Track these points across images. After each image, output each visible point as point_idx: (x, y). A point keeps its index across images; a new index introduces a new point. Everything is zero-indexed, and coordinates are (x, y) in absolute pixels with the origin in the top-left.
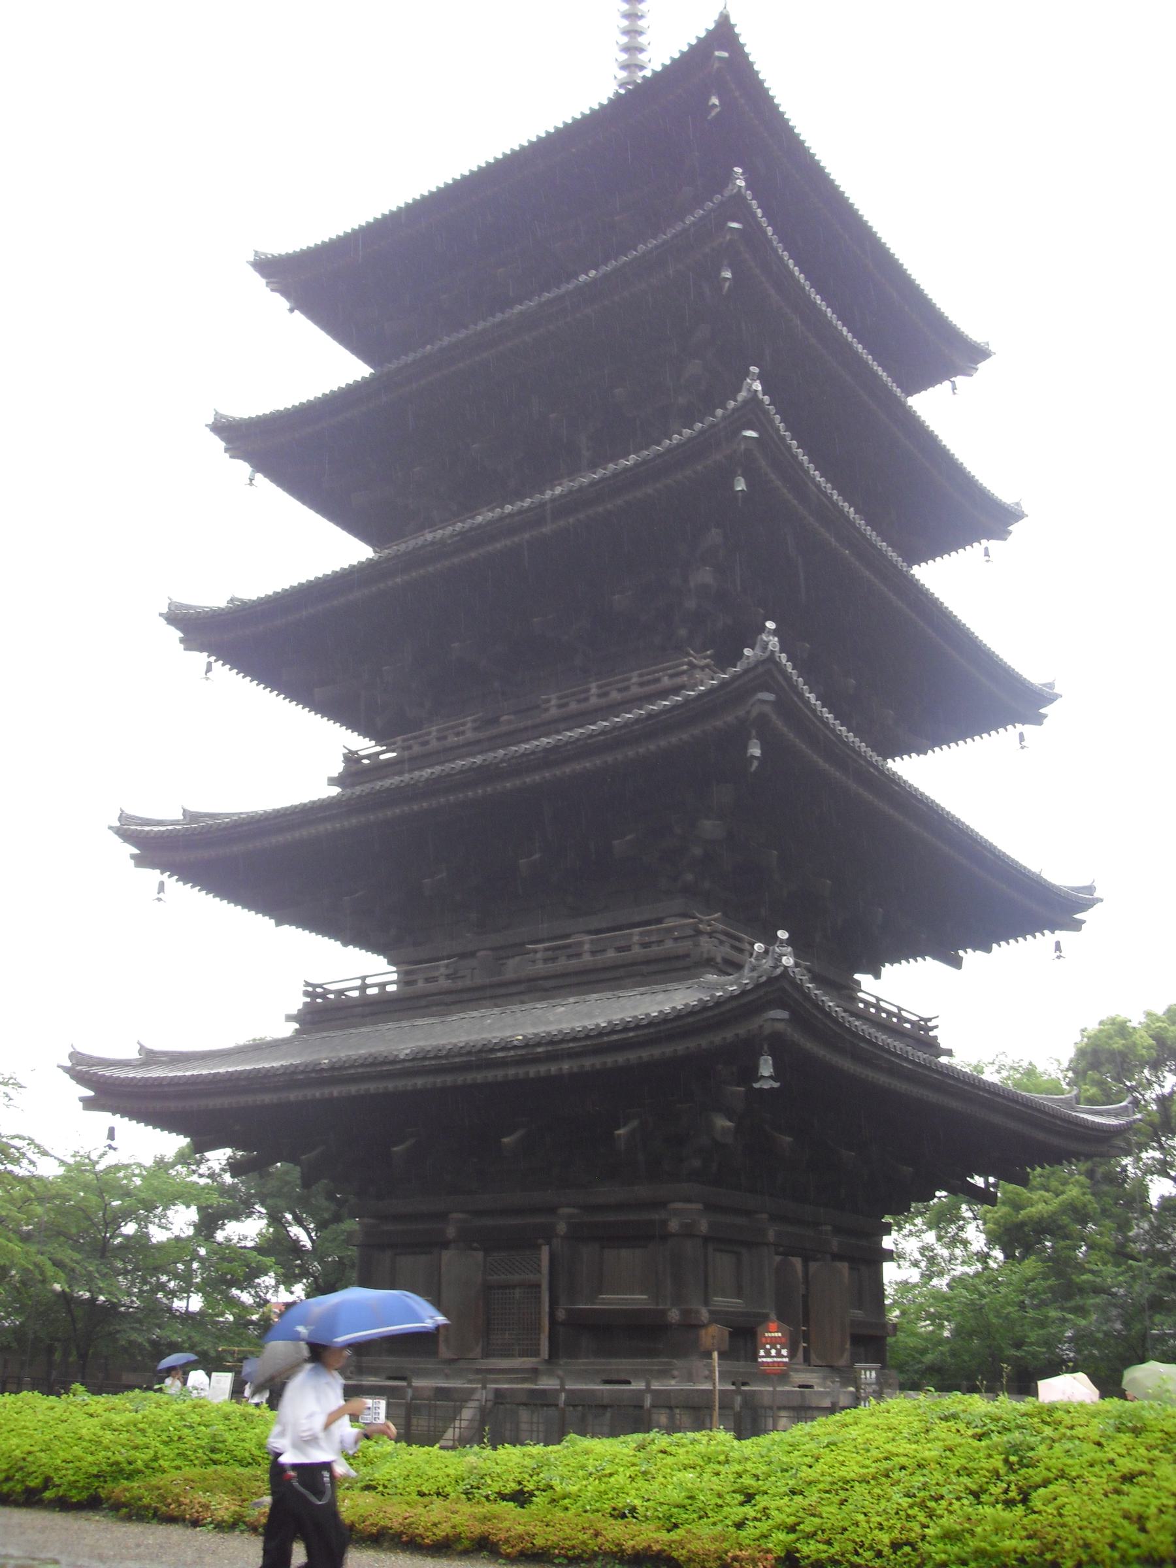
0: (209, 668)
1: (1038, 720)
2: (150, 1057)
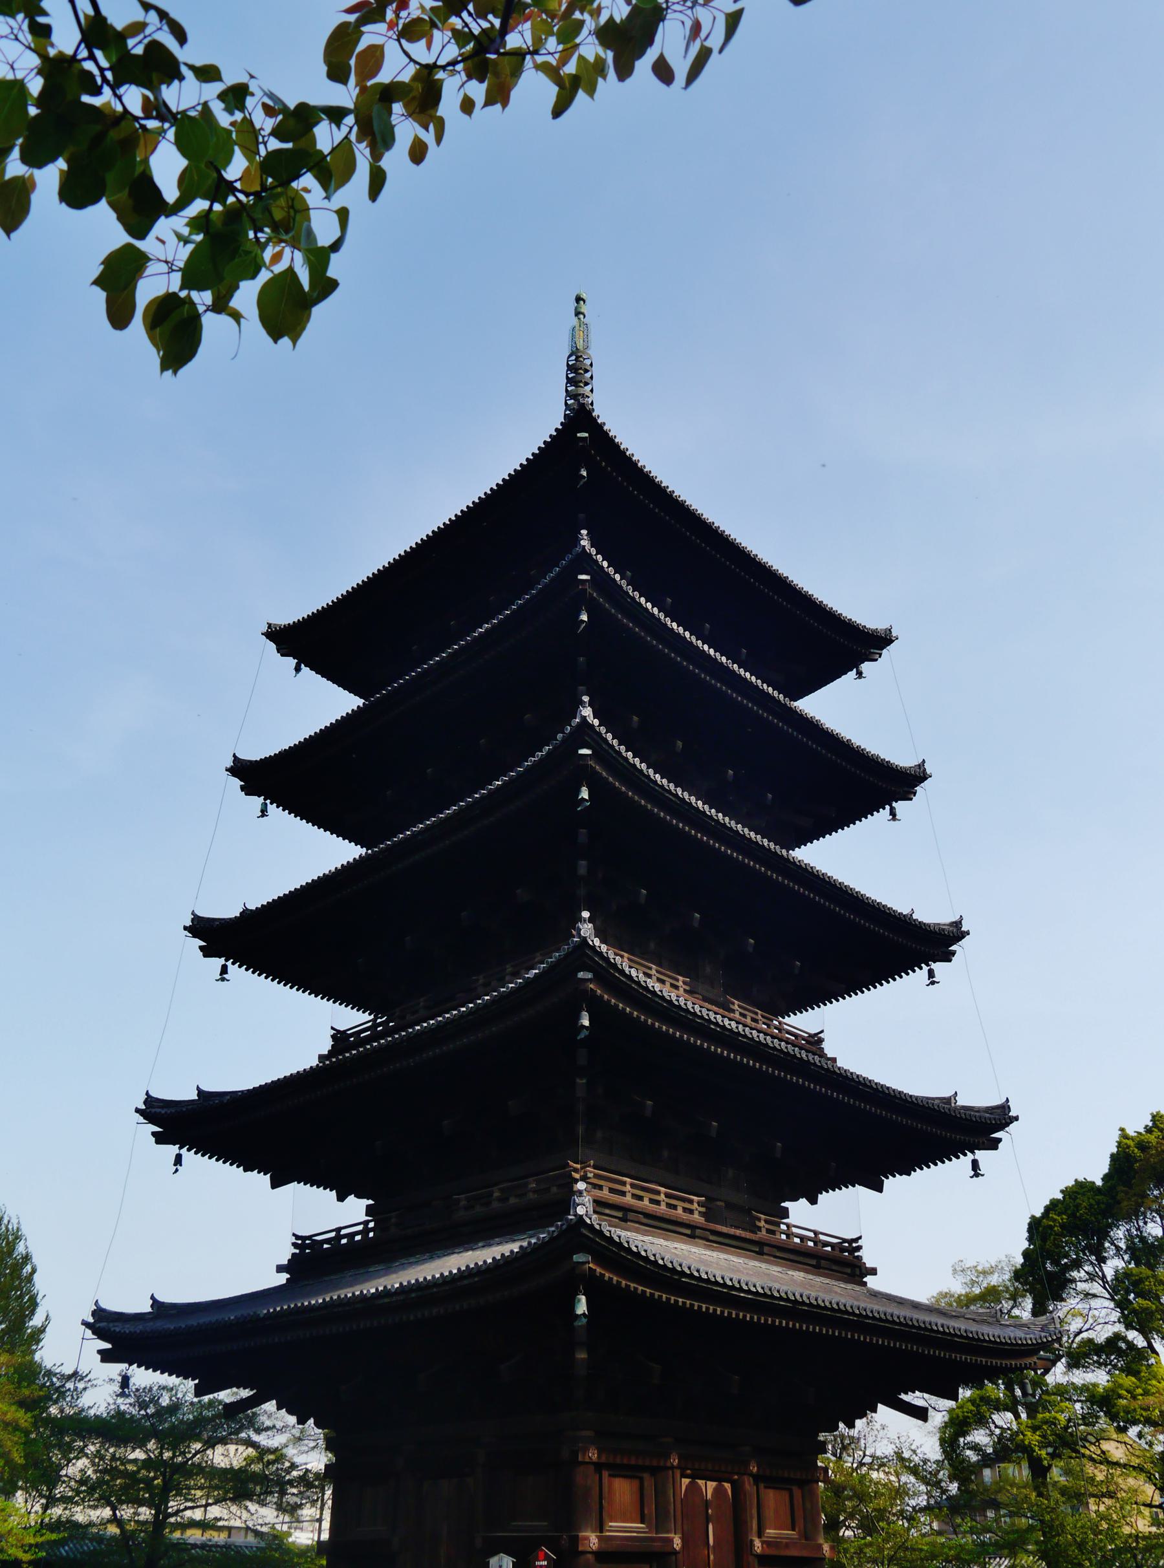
0: (224, 970)
1: (947, 957)
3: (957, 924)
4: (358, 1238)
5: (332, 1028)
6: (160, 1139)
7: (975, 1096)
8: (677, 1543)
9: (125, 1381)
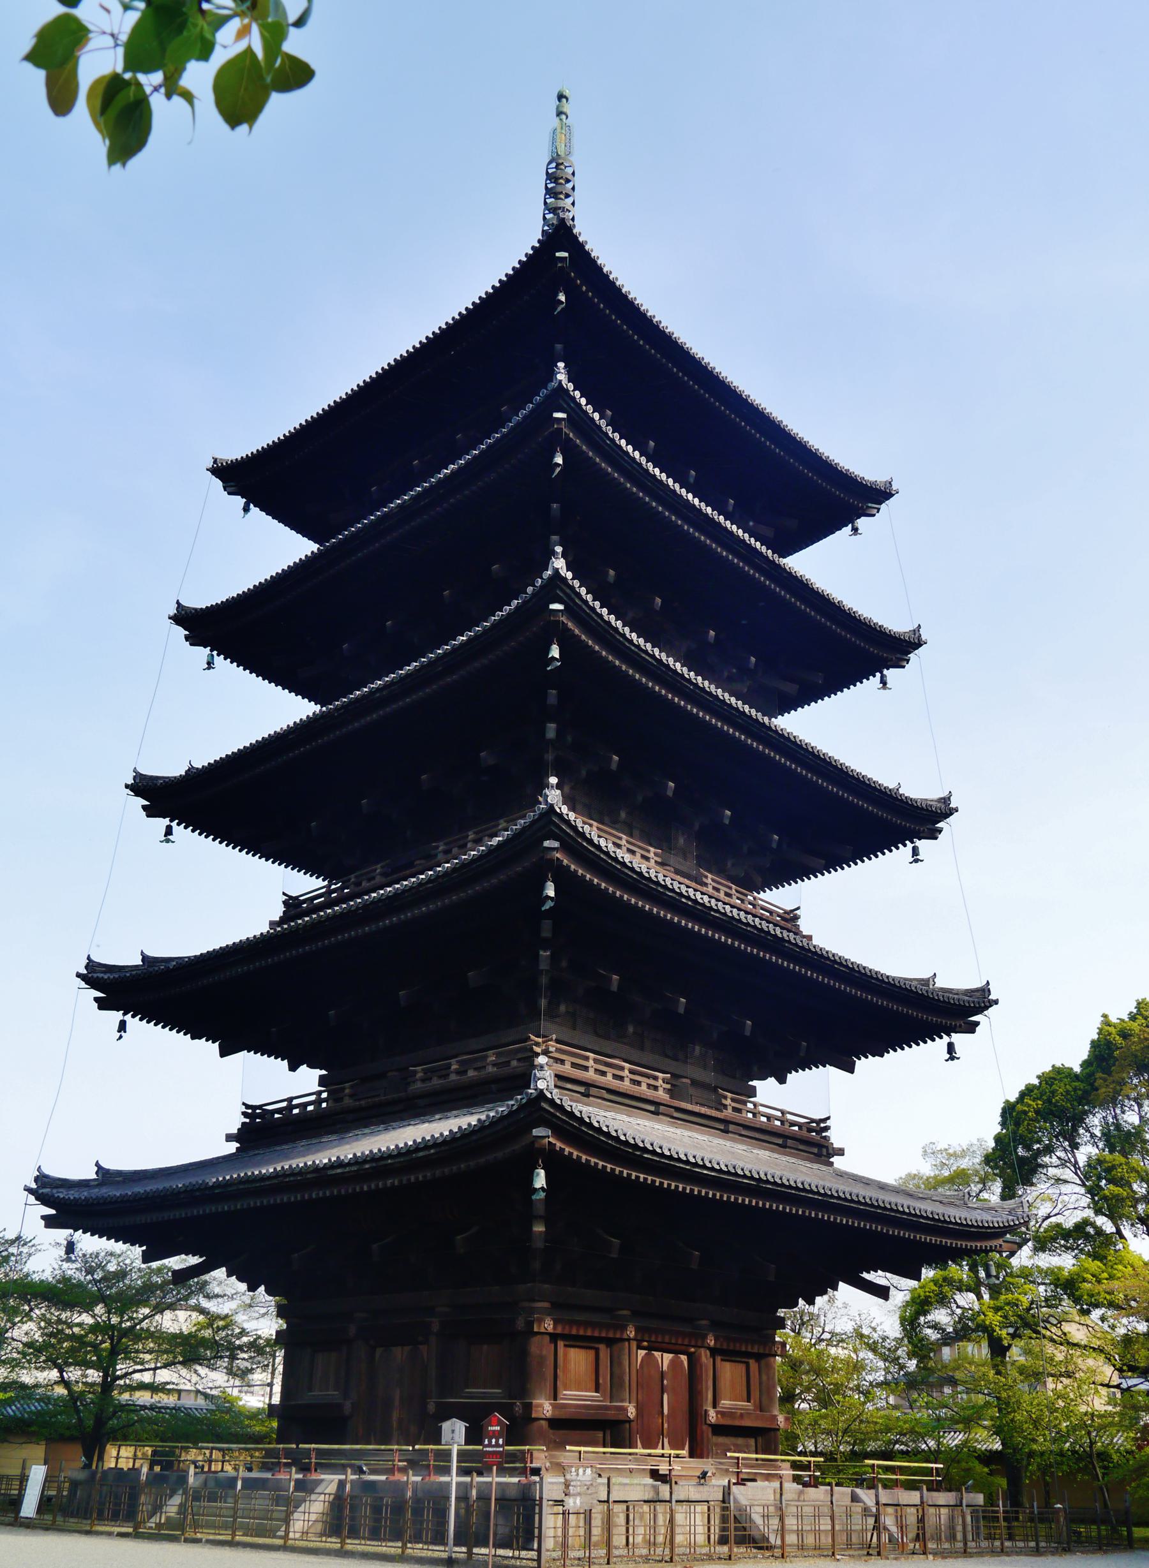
0: (169, 831)
1: (933, 834)
2: (105, 1176)
3: (946, 800)
4: (310, 1108)
5: (284, 894)
6: (102, 1004)
7: (954, 978)
8: (632, 1412)
9: (70, 1247)
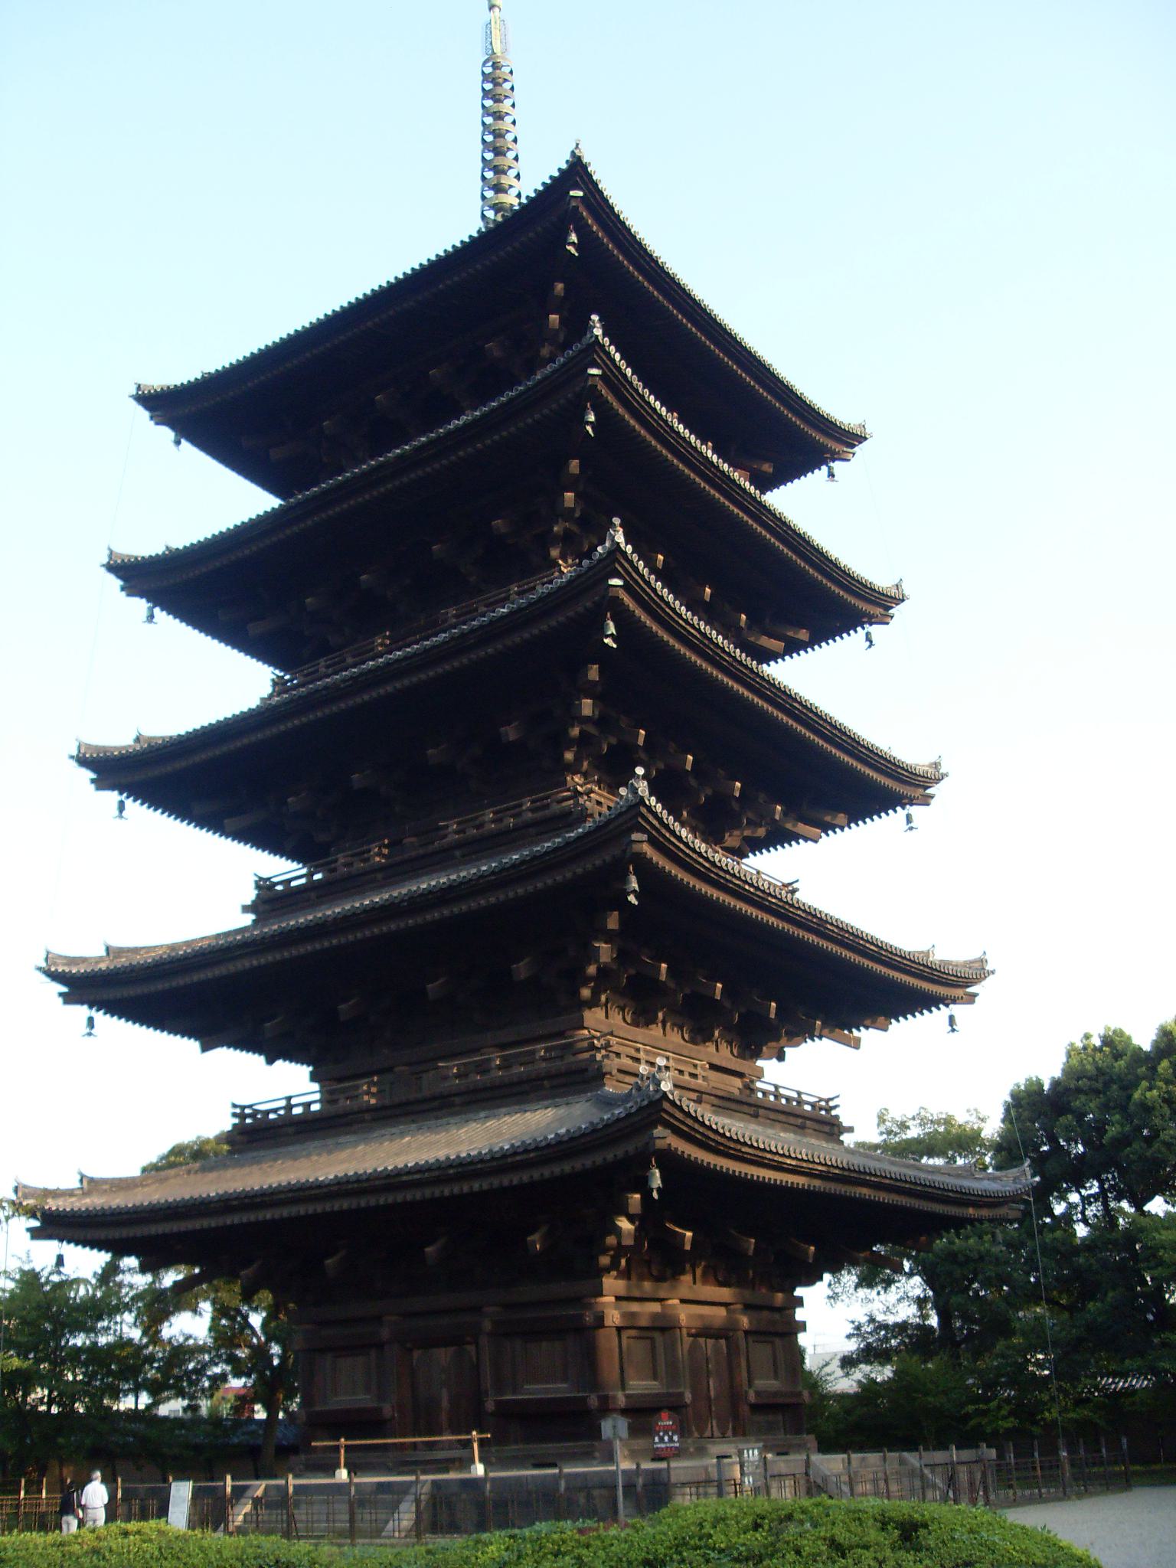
0: (121, 806)
1: (926, 800)
2: (92, 1185)
3: (936, 765)
6: (68, 999)
